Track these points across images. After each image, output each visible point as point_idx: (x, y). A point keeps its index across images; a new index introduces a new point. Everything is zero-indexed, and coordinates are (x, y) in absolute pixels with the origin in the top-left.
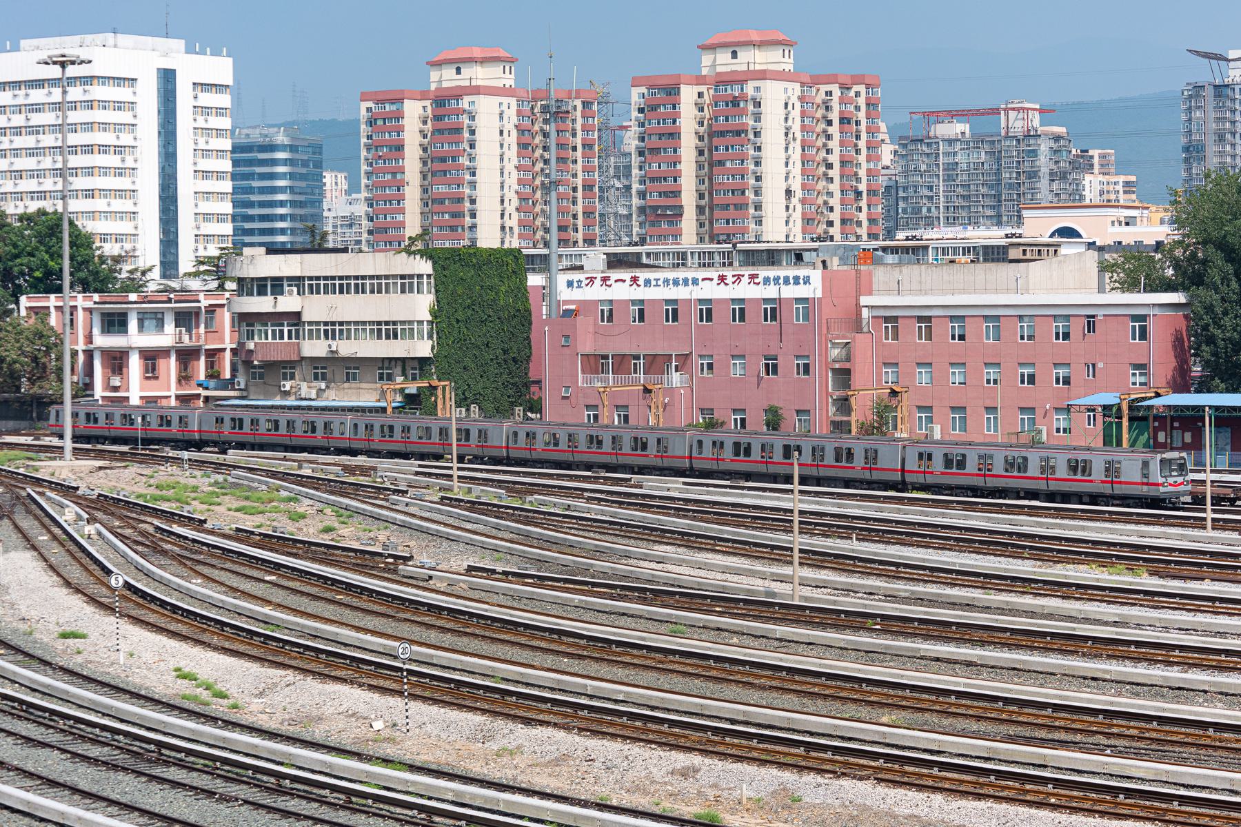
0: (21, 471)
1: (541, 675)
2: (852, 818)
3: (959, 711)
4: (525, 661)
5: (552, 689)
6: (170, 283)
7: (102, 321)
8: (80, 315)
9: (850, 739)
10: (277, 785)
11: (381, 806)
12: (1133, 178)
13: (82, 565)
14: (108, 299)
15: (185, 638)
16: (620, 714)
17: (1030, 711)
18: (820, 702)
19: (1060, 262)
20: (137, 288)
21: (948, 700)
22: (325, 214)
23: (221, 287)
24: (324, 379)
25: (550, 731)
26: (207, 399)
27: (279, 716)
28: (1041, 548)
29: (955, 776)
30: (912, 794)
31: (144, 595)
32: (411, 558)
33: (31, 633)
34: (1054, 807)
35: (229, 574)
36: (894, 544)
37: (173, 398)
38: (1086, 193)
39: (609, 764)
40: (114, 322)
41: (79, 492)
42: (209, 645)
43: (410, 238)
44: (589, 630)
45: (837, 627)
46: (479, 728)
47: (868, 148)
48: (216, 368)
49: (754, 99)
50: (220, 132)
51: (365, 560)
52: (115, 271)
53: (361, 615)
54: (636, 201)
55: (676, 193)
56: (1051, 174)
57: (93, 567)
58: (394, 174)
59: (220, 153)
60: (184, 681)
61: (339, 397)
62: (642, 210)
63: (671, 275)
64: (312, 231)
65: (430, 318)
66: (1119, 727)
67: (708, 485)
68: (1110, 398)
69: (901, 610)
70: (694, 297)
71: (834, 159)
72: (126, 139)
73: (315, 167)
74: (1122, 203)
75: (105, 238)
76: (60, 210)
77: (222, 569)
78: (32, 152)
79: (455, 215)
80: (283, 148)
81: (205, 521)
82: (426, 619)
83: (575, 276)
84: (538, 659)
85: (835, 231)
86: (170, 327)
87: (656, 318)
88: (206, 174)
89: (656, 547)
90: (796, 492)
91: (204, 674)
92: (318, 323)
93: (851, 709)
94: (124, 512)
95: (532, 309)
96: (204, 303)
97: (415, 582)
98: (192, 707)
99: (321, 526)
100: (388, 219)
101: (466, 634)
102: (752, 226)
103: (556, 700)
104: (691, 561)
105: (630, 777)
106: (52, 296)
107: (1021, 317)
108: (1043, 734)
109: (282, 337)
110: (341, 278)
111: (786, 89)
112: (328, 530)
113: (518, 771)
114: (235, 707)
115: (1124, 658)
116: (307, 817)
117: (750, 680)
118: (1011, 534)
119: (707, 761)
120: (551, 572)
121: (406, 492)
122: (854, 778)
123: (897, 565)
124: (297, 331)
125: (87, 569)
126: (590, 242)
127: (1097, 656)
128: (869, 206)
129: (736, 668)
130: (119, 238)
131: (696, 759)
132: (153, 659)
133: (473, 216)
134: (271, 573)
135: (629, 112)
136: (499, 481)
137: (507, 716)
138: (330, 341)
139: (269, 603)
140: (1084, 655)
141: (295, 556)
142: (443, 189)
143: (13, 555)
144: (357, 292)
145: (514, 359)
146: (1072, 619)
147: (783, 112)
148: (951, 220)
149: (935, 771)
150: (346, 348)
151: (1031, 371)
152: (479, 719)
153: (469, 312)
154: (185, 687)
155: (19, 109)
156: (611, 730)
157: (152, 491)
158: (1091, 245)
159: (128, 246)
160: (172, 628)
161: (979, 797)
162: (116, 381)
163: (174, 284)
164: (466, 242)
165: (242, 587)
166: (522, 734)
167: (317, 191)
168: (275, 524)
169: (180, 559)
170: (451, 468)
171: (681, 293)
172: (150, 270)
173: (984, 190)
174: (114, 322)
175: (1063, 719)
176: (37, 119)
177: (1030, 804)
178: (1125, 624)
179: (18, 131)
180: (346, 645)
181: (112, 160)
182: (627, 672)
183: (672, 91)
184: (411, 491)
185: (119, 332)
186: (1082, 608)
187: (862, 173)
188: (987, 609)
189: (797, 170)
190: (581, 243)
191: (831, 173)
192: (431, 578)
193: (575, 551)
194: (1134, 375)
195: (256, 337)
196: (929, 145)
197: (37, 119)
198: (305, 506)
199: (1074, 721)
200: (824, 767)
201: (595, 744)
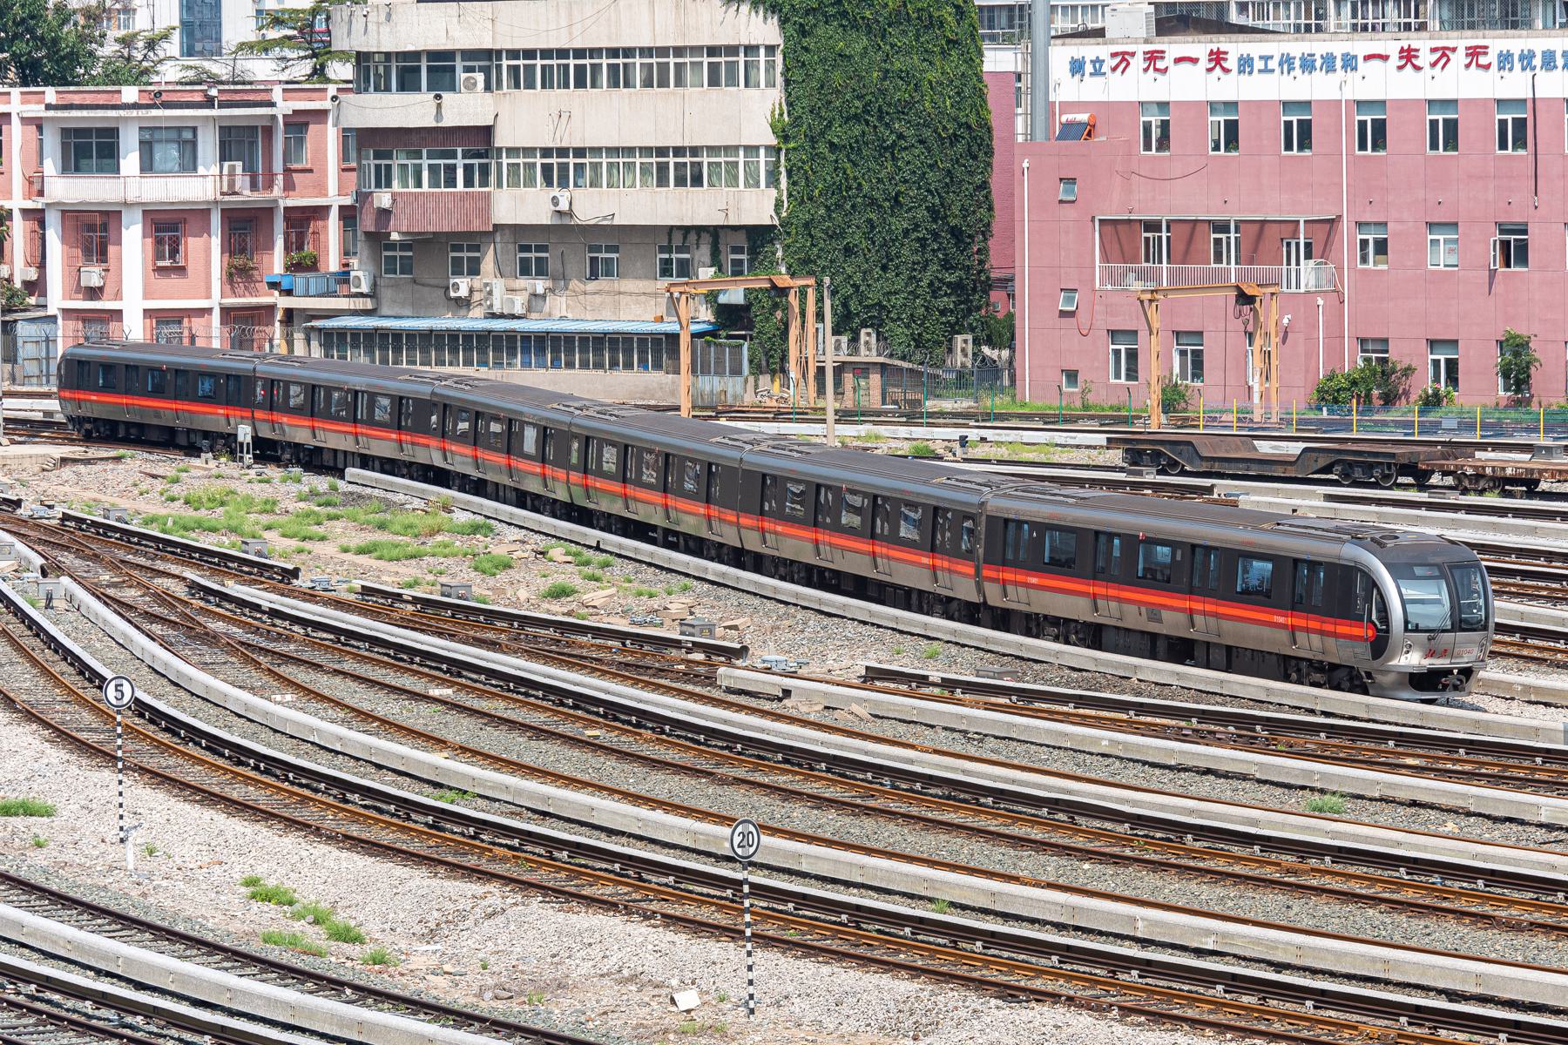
1: (1037, 895)
4: (998, 869)
5: (1060, 927)
6: (207, 65)
7: (65, 147)
13: (34, 662)
14: (77, 99)
15: (268, 816)
16: (1210, 978)
20: (139, 76)
23: (319, 72)
24: (542, 271)
26: (289, 314)
27: (474, 978)
31: (174, 726)
32: (743, 652)
35: (353, 685)
37: (216, 315)
41: (23, 512)
42: (317, 831)
44: (1135, 803)
46: (905, 1006)
48: (309, 249)
51: (643, 654)
53: (640, 770)
57: (61, 668)
60: (266, 907)
61: (575, 309)
63: (1298, 47)
65: (773, 141)
77: (337, 672)
81: (295, 573)
82: (781, 780)
83: (1089, 50)
84: (1027, 863)
87: (1261, 137)
91: (308, 892)
92: (529, 151)
94: (121, 554)
95: (995, 121)
96: (284, 107)
97: (753, 702)
98: (287, 958)
103: (1069, 948)
109: (451, 182)
110: (580, 53)
112: (559, 593)
114: (379, 960)
117: (1487, 909)
120: (1046, 681)
124: (485, 170)
125: (46, 672)
129: (1456, 885)
137: (966, 981)
139: (441, 743)
145: (956, 233)
150: (593, 205)
152: (904, 986)
153: (857, 130)
154: (267, 917)
156: (1190, 1013)
157: (177, 509)
160: (235, 796)
162: (92, 276)
163: (218, 68)
165: (381, 711)
168: (444, 580)
169: (246, 653)
180: (611, 832)
182: (1219, 891)
185: (100, 170)
192: (787, 693)
195: (395, 183)
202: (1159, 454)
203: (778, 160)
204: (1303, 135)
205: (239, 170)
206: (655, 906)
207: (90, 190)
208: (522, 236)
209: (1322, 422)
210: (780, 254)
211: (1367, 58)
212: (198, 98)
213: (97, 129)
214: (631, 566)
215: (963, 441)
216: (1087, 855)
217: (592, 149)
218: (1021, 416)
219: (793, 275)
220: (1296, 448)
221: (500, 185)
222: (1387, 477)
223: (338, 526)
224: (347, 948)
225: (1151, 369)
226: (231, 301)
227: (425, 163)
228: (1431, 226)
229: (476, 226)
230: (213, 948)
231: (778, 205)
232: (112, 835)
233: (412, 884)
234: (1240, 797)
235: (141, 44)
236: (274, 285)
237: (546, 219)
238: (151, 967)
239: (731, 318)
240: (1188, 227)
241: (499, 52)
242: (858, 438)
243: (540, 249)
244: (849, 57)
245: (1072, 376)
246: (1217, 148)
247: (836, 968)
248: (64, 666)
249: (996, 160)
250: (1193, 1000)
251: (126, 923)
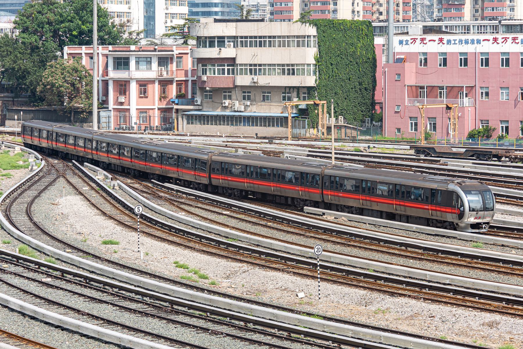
6: (154, 40)
7: (114, 62)
13: (111, 203)
14: (118, 49)
20: (135, 43)
23: (185, 43)
35: (201, 210)
40: (122, 63)
57: (118, 205)
63: (464, 37)
65: (314, 62)
70: (478, 51)
86: (155, 65)
92: (246, 65)
96: (176, 52)
106: (84, 47)
124: (233, 70)
125: (114, 206)
134: (226, 210)
138: (253, 76)
143: (69, 197)
144: (270, 46)
145: (366, 89)
150: (263, 80)
153: (339, 59)
169: (170, 202)
170: (331, 153)
171: (469, 49)
172: (141, 32)
174: (122, 63)
185: (124, 69)
195: (208, 73)
202: (425, 151)
203: (316, 68)
204: (465, 62)
205: (163, 70)
207: (121, 75)
208: (244, 89)
209: (470, 143)
210: (316, 94)
211: (484, 40)
212: (152, 49)
213: (124, 58)
215: (369, 147)
217: (264, 64)
218: (385, 141)
219: (320, 100)
220: (463, 150)
221: (237, 74)
222: (490, 158)
225: (421, 128)
229: (231, 86)
231: (316, 81)
235: (135, 34)
239: (303, 113)
241: (237, 37)
242: (339, 146)
245: (399, 130)
246: (440, 65)
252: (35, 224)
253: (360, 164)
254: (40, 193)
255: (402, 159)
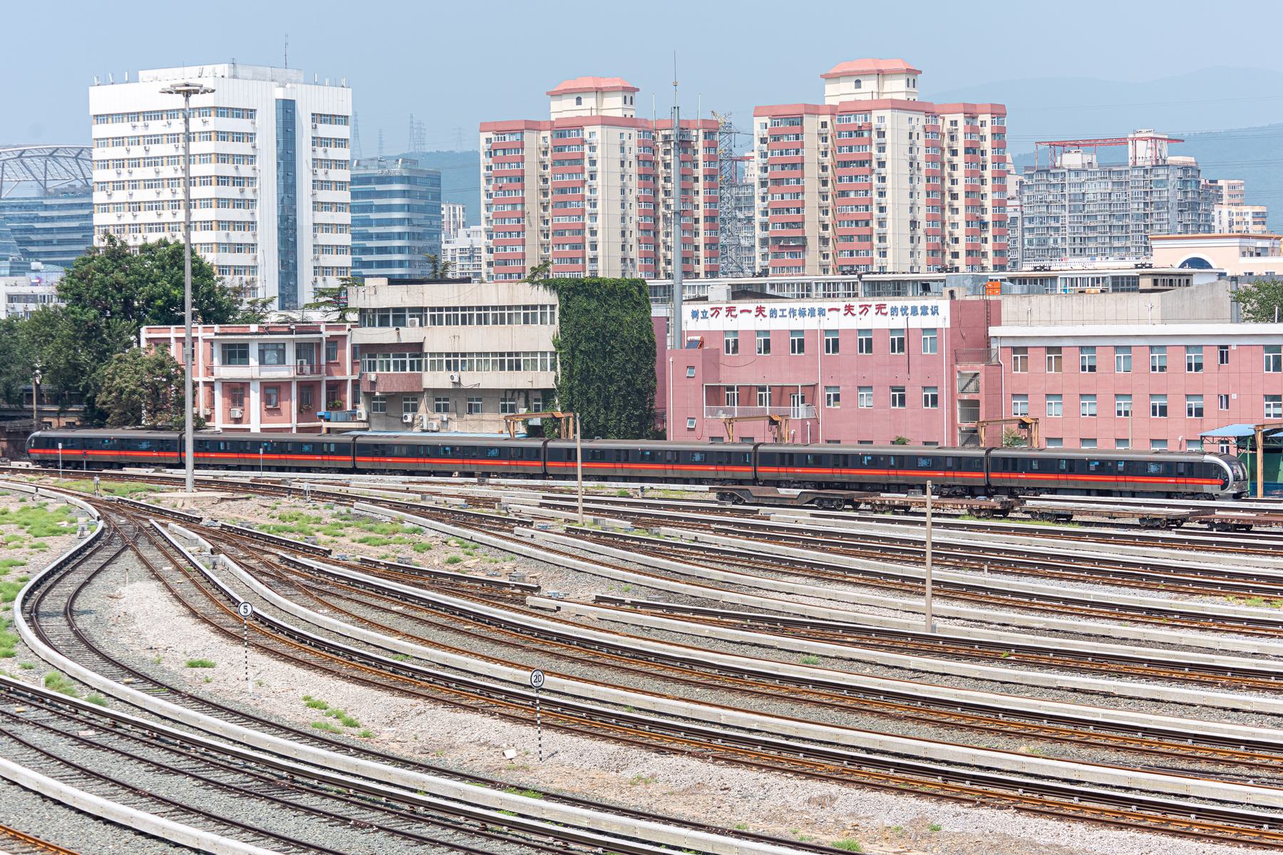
0: (143, 502)
2: (993, 847)
3: (1097, 741)
5: (685, 719)
6: (290, 314)
7: (223, 353)
8: (200, 346)
9: (989, 769)
10: (407, 812)
11: (517, 833)
12: (1263, 209)
13: (207, 595)
14: (229, 330)
16: (755, 743)
17: (1169, 741)
18: (956, 732)
19: (1192, 292)
21: (1085, 730)
22: (444, 246)
23: (342, 317)
24: (446, 410)
25: (684, 760)
26: (329, 430)
27: (411, 744)
28: (1176, 580)
29: (1096, 805)
30: (1053, 824)
31: (272, 625)
33: (159, 662)
34: (1198, 837)
36: (1027, 575)
38: (1215, 224)
39: (744, 793)
40: (235, 353)
42: (338, 675)
43: (533, 269)
45: (969, 657)
46: (613, 757)
47: (994, 178)
49: (878, 129)
50: (340, 164)
51: (492, 591)
52: (236, 302)
54: (759, 233)
55: (800, 225)
56: (1180, 205)
58: (514, 205)
59: (341, 185)
60: (314, 710)
62: (764, 242)
63: (797, 305)
64: (434, 262)
66: (1261, 757)
67: (836, 517)
68: (1246, 430)
69: (1036, 641)
71: (960, 189)
72: (245, 170)
73: (433, 198)
74: (1251, 233)
75: (223, 269)
76: (182, 241)
78: (150, 184)
79: (575, 247)
80: (401, 179)
81: (330, 552)
83: (700, 307)
84: (670, 688)
85: (961, 262)
88: (326, 206)
89: (786, 578)
90: (929, 524)
91: (333, 705)
92: (440, 354)
93: (989, 739)
94: (248, 543)
95: (656, 340)
96: (326, 334)
97: (543, 613)
99: (446, 557)
100: (508, 251)
101: (595, 664)
102: (876, 257)
104: (821, 593)
105: (767, 805)
106: (173, 327)
107: (1151, 347)
108: (1183, 764)
109: (404, 369)
110: (463, 309)
111: (910, 119)
113: (653, 800)
115: (1265, 689)
116: (442, 843)
117: (885, 710)
118: (1145, 566)
119: (844, 789)
121: (531, 524)
122: (993, 807)
123: (1031, 596)
124: (419, 363)
125: (212, 599)
126: (712, 273)
127: (1237, 688)
128: (995, 237)
129: (871, 698)
130: (238, 270)
131: (833, 788)
132: (285, 688)
133: (594, 247)
134: (398, 604)
135: (751, 142)
136: (624, 513)
137: (641, 745)
138: (452, 373)
139: (396, 632)
140: (1223, 686)
141: (421, 586)
142: (564, 220)
143: (138, 584)
144: (479, 323)
145: (639, 391)
146: (1210, 650)
147: (907, 142)
148: (1077, 252)
149: (1076, 800)
150: (469, 379)
151: (1163, 402)
152: (612, 747)
154: (314, 715)
155: (137, 140)
156: (746, 759)
157: (276, 522)
158: (1222, 275)
159: (247, 278)
160: (300, 658)
161: (1121, 826)
162: (237, 413)
163: (296, 315)
164: (588, 274)
166: (657, 763)
167: (435, 223)
169: (306, 590)
170: (576, 500)
172: (271, 301)
173: (1115, 222)
175: (1204, 749)
176: (156, 150)
177: (1174, 833)
178: (1263, 656)
179: (136, 162)
180: (476, 674)
181: (232, 192)
182: (760, 701)
183: (796, 120)
184: (537, 523)
185: (240, 363)
186: (1220, 639)
187: (988, 203)
188: (1124, 640)
189: (922, 200)
190: (702, 275)
191: (956, 204)
192: (559, 608)
193: (704, 582)
194: (1268, 406)
196: (1054, 175)
197: (156, 150)
198: (428, 537)
199: (1215, 752)
200: (962, 796)
201: (730, 773)
202: (732, 495)
206: (496, 709)
211: (830, 310)
214: (487, 548)
215: (642, 489)
216: (697, 684)
223: (350, 530)
224: (352, 730)
226: (301, 425)
227: (392, 360)
228: (860, 388)
230: (289, 730)
232: (243, 676)
233: (382, 699)
234: (770, 657)
236: (321, 417)
237: (451, 387)
238: (260, 740)
240: (747, 390)
243: (445, 399)
244: (588, 311)
247: (580, 738)
248: (221, 596)
249: (657, 358)
250: (746, 753)
251: (248, 718)
252: (77, 633)
253: (625, 519)
254: (90, 578)
255: (696, 509)
